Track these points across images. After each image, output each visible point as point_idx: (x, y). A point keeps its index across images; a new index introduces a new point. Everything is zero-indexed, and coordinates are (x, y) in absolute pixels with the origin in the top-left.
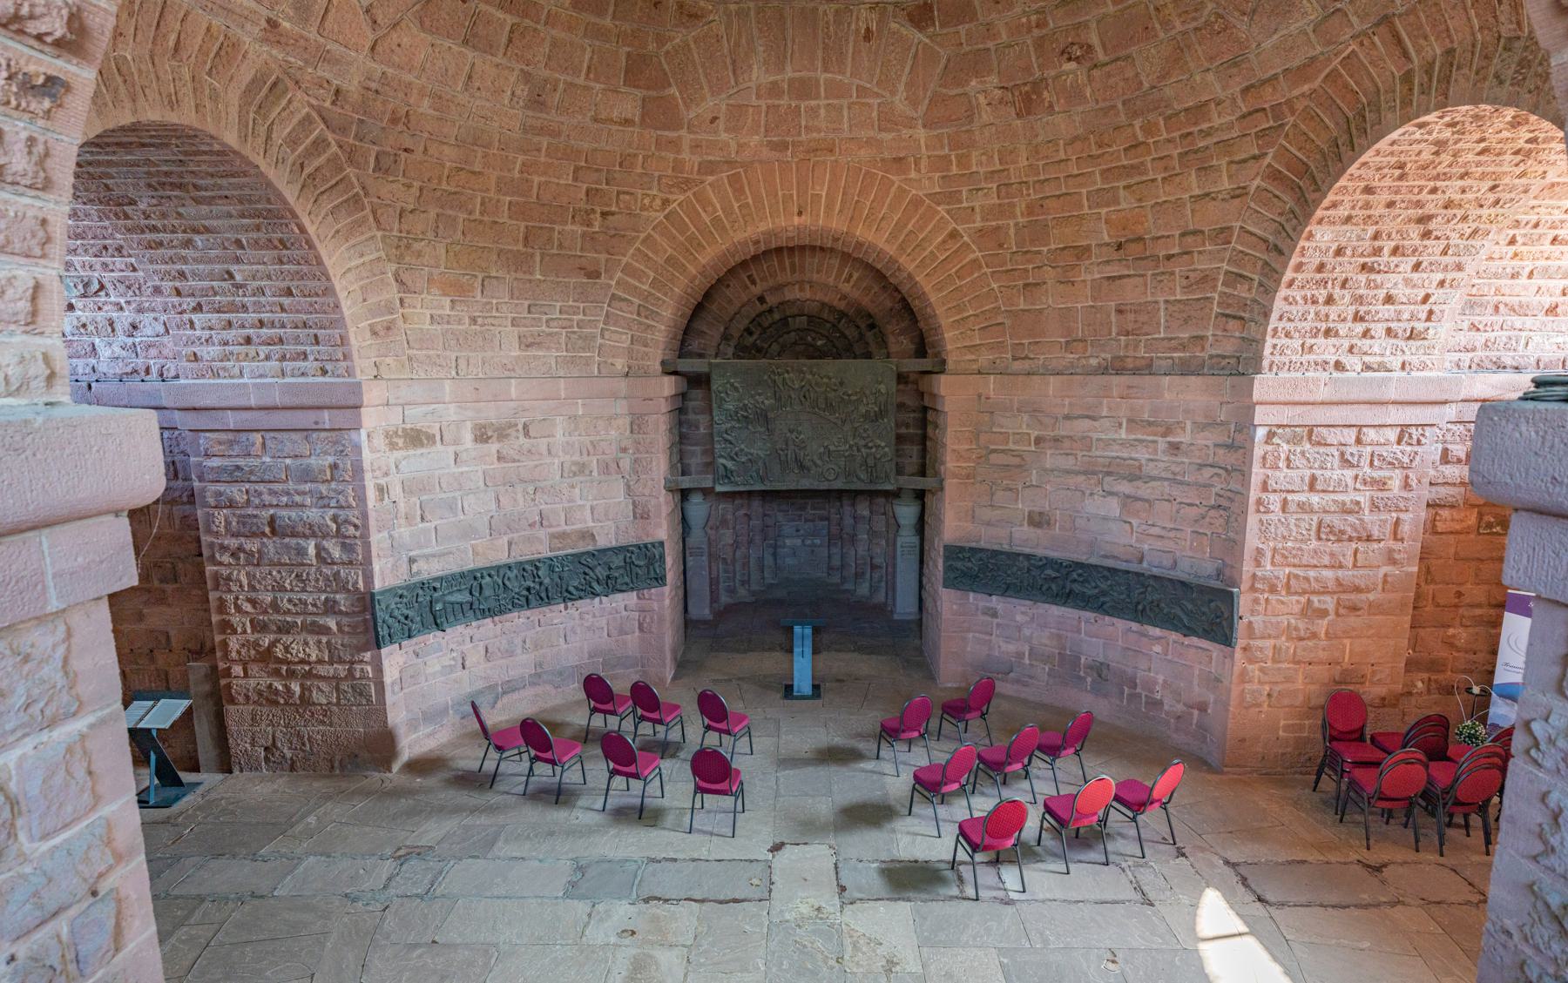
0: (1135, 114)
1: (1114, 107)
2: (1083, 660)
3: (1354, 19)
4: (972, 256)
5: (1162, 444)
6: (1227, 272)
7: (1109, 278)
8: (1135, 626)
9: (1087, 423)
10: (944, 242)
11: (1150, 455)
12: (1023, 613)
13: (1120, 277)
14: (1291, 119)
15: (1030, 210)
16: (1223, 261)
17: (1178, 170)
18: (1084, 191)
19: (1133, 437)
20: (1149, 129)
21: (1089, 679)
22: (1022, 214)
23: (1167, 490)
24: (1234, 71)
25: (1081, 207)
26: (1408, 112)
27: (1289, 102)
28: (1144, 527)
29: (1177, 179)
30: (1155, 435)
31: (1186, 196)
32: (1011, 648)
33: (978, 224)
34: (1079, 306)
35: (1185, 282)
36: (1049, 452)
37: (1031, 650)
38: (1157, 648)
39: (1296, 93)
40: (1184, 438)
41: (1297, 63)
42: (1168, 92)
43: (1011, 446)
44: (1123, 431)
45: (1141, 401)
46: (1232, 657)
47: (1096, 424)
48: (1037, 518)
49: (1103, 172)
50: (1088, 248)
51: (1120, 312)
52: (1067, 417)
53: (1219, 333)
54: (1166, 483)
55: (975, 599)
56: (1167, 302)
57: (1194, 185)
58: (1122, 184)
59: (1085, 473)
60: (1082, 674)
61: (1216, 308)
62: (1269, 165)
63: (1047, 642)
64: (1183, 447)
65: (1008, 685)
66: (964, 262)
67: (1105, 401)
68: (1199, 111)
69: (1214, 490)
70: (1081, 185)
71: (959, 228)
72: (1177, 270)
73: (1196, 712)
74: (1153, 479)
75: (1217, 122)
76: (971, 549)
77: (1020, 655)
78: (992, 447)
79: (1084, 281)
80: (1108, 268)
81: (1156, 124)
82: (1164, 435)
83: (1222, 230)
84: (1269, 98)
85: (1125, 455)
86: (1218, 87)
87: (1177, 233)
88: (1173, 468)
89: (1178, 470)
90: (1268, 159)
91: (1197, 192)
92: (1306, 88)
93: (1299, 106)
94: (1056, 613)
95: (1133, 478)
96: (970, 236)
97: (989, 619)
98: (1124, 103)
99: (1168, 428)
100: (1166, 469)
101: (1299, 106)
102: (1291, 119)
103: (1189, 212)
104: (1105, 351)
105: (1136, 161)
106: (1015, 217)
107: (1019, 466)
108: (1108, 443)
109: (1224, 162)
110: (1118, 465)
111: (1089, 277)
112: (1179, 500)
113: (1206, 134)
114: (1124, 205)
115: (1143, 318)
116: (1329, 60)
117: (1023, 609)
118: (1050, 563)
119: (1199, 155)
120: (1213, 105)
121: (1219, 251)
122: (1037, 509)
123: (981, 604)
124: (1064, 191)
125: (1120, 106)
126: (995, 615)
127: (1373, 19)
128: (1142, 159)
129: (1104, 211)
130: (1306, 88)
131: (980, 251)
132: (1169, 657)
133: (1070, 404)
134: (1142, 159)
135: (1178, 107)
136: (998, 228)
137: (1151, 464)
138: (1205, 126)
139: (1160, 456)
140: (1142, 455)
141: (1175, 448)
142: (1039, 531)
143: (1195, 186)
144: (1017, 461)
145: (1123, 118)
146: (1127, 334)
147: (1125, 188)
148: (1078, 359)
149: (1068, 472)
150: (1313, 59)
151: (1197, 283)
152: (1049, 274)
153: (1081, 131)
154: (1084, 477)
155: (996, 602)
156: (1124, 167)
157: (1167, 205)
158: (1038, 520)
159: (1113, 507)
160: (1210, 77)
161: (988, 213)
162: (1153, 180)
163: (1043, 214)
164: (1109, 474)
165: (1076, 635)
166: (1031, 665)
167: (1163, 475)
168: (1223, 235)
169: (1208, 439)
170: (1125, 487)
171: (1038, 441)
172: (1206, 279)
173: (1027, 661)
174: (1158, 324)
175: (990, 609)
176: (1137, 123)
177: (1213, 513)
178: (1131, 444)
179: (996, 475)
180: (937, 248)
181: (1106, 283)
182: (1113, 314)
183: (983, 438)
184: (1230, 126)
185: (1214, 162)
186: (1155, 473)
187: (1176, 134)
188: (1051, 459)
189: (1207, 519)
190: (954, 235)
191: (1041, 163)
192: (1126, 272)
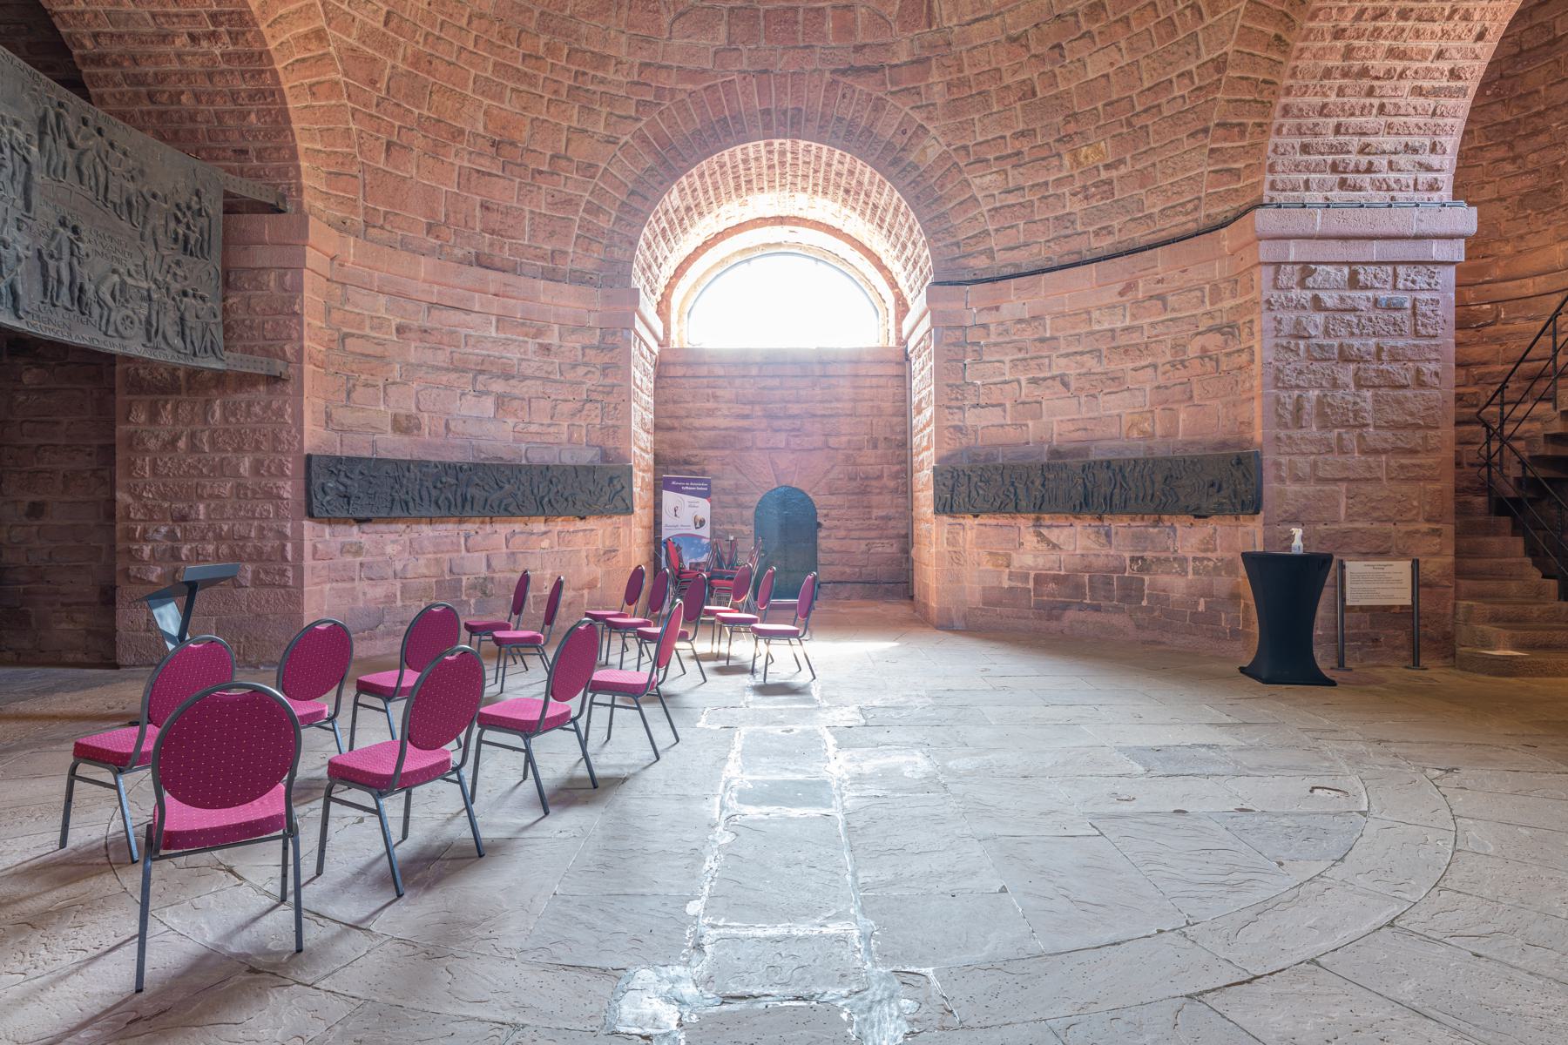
0: (546, 29)
1: (532, 11)
2: (464, 584)
3: (745, 61)
4: (333, 76)
5: (532, 345)
6: (588, 202)
7: (478, 171)
8: (518, 527)
9: (460, 316)
10: (306, 36)
11: (520, 352)
12: (393, 542)
13: (490, 174)
14: (667, 103)
15: (416, 60)
16: (586, 191)
17: (564, 98)
18: (473, 71)
19: (503, 336)
20: (551, 49)
21: (472, 601)
22: (404, 59)
23: (541, 389)
24: (647, 46)
25: (465, 86)
26: (768, 133)
27: (672, 90)
28: (522, 425)
29: (564, 107)
30: (526, 335)
31: (565, 124)
32: (379, 591)
33: (353, 42)
34: (444, 188)
35: (550, 200)
36: (413, 345)
37: (404, 586)
38: (546, 543)
39: (680, 86)
40: (553, 339)
41: (691, 66)
42: (584, 30)
43: (367, 331)
44: (493, 329)
45: (513, 301)
46: (628, 524)
47: (468, 318)
48: (405, 423)
49: (495, 64)
50: (461, 132)
51: (485, 207)
52: (432, 306)
53: (579, 251)
54: (539, 382)
55: (333, 535)
56: (532, 212)
57: (575, 117)
58: (511, 85)
59: (456, 370)
60: (464, 598)
61: (576, 231)
62: (640, 129)
63: (426, 572)
64: (554, 349)
65: (379, 643)
66: (323, 78)
67: (477, 295)
68: (602, 60)
69: (585, 387)
70: (472, 64)
71: (328, 31)
72: (544, 186)
73: (586, 592)
74: (525, 378)
75: (611, 76)
76: (349, 459)
77: (390, 598)
78: (345, 330)
79: (452, 164)
80: (482, 161)
81: (561, 50)
82: (535, 337)
83: (590, 165)
84: (669, 81)
85: (497, 354)
86: (624, 50)
87: (549, 153)
88: (545, 367)
89: (550, 369)
90: (640, 125)
91: (575, 124)
92: (689, 87)
93: (678, 98)
94: (431, 534)
95: (507, 376)
96: (338, 50)
97: (349, 558)
98: (542, 14)
99: (538, 330)
100: (539, 368)
101: (678, 98)
102: (667, 103)
103: (564, 140)
104: (469, 245)
105: (530, 71)
106: (395, 57)
107: (382, 357)
108: (480, 340)
109: (605, 110)
110: (492, 363)
111: (458, 162)
112: (553, 397)
113: (602, 81)
114: (506, 106)
115: (510, 221)
116: (716, 77)
117: (393, 537)
118: (448, 467)
119: (588, 95)
120: (613, 62)
121: (584, 182)
122: (403, 412)
123: (341, 539)
124: (454, 60)
125: (537, 14)
126: (358, 550)
127: (758, 68)
128: (536, 72)
129: (487, 102)
130: (689, 87)
131: (346, 74)
132: (556, 549)
133: (439, 293)
134: (536, 72)
135: (584, 46)
136: (374, 60)
137: (524, 364)
138: (600, 74)
139: (530, 355)
140: (513, 355)
141: (546, 349)
142: (406, 439)
143: (574, 118)
144: (379, 350)
145: (533, 25)
146: (493, 233)
147: (513, 90)
148: (441, 246)
149: (438, 369)
150: (704, 71)
151: (562, 203)
152: (419, 141)
153: (489, 11)
154: (457, 375)
155: (354, 534)
156: (518, 70)
157: (546, 125)
158: (404, 425)
159: (489, 403)
160: (624, 39)
161: (367, 35)
162: (541, 96)
163: (429, 73)
164: (481, 372)
165: (455, 555)
166: (404, 606)
167: (536, 374)
168: (588, 169)
169: (574, 343)
170: (498, 386)
171: (400, 330)
172: (569, 202)
173: (399, 603)
174: (524, 230)
175: (351, 544)
176: (544, 38)
177: (588, 406)
178: (506, 343)
179: (354, 367)
180: (296, 38)
181: (475, 175)
182: (478, 208)
183: (336, 315)
184: (620, 85)
185: (596, 107)
186: (529, 372)
187: (574, 68)
188: (415, 352)
189: (585, 412)
190: (319, 35)
191: (441, 17)
192: (494, 172)
